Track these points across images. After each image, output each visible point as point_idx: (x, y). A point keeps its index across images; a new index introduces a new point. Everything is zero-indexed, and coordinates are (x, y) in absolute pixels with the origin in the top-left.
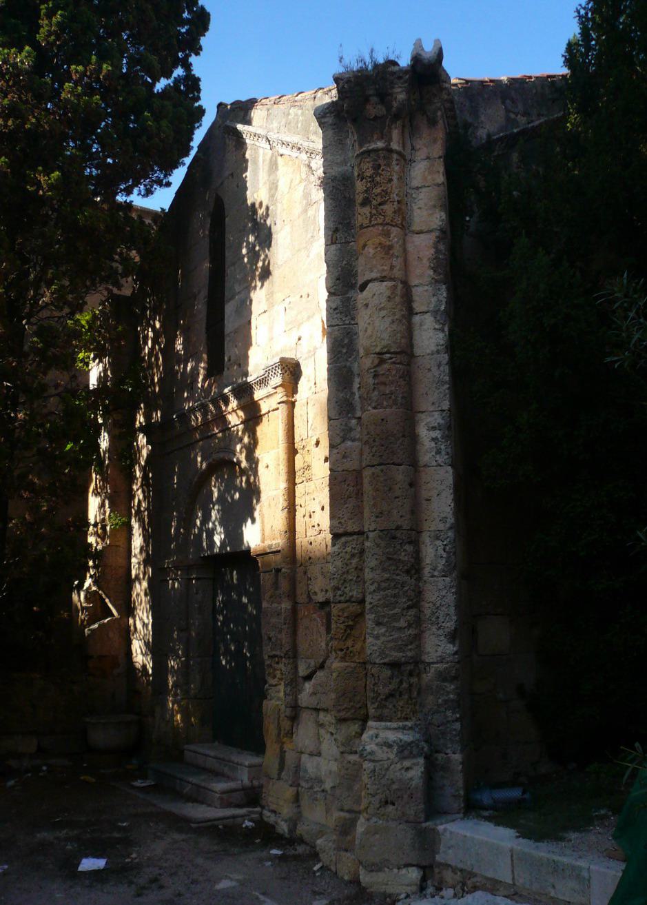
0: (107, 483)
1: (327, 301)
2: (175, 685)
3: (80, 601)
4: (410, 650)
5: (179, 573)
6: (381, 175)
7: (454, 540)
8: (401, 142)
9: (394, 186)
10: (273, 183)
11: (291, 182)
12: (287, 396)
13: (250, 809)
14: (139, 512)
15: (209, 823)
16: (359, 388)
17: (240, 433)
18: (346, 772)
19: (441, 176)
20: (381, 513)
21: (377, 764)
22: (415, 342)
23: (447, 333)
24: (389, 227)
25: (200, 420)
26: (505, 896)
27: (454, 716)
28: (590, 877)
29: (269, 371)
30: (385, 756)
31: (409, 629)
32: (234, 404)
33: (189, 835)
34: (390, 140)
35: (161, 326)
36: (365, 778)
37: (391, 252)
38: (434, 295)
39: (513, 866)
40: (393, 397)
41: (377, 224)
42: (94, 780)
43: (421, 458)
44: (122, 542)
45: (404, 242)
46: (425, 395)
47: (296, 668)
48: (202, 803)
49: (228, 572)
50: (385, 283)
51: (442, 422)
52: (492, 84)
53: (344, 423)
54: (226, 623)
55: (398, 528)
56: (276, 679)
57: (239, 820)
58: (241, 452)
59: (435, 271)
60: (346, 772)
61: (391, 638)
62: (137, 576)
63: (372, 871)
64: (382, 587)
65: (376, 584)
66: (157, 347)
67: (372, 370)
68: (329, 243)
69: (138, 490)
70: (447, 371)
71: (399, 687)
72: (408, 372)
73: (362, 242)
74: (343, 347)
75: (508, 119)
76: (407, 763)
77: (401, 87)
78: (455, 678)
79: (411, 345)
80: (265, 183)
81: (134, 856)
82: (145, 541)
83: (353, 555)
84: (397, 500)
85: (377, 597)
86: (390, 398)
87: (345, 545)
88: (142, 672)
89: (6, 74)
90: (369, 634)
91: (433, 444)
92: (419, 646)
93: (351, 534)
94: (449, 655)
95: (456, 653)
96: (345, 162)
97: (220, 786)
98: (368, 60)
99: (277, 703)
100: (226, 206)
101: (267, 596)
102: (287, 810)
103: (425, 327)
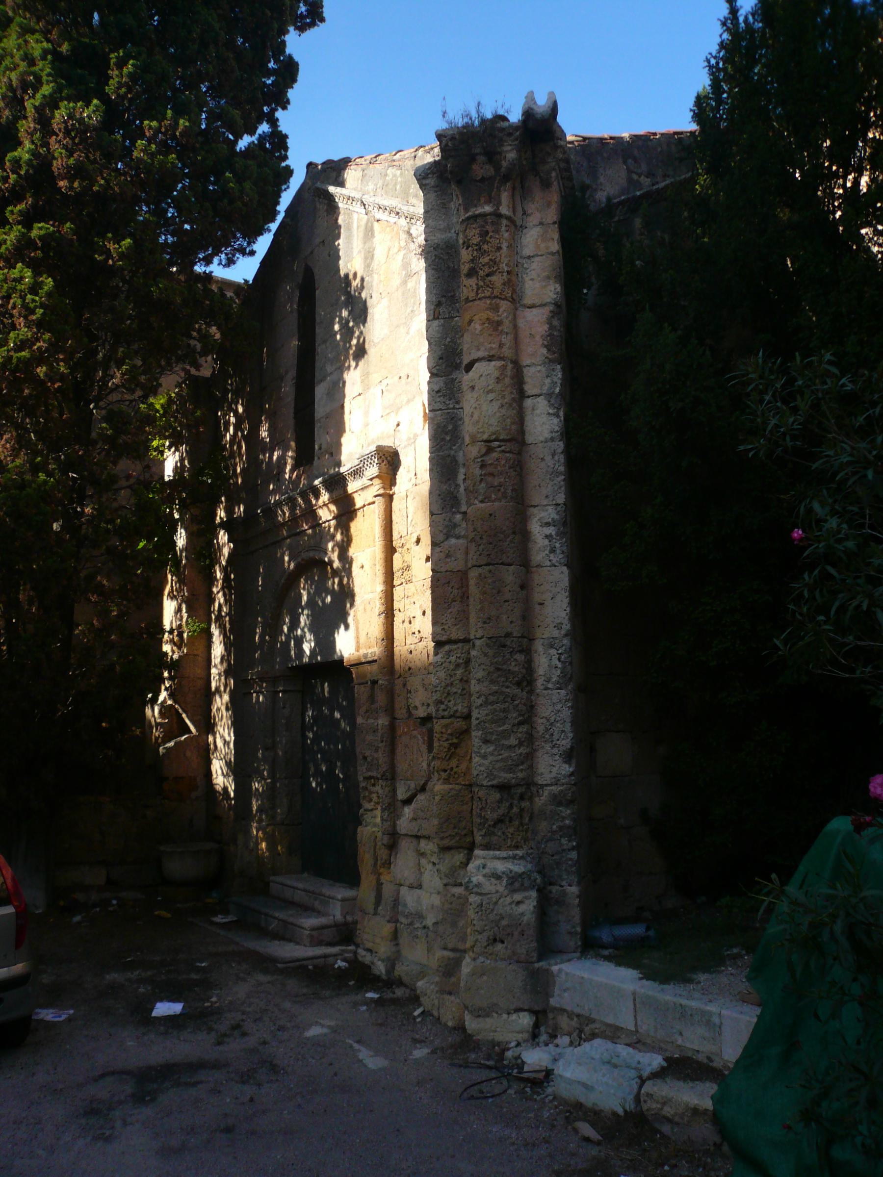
0: (185, 584)
1: (429, 383)
2: (260, 810)
3: (153, 715)
4: (522, 770)
6: (488, 242)
7: (570, 649)
8: (511, 206)
9: (503, 255)
10: (369, 252)
11: (389, 250)
12: (384, 488)
13: (344, 948)
14: (219, 618)
16: (465, 479)
17: (332, 530)
20: (489, 619)
21: (485, 898)
23: (562, 418)
24: (498, 301)
25: (287, 515)
28: (721, 1023)
29: (364, 460)
30: (493, 889)
32: (325, 497)
34: (499, 204)
35: (244, 411)
36: (471, 913)
37: (500, 328)
38: (547, 376)
41: (485, 297)
42: (169, 916)
43: (533, 558)
44: (200, 649)
45: (515, 317)
46: (538, 487)
47: (394, 791)
48: (290, 940)
49: (319, 685)
50: (493, 363)
51: (556, 517)
52: (612, 141)
53: (447, 519)
55: (508, 635)
56: (372, 803)
57: (331, 960)
59: (549, 350)
61: (500, 757)
62: (217, 689)
63: (479, 1016)
64: (490, 701)
65: (483, 698)
66: (240, 434)
67: (479, 460)
68: (431, 318)
69: (218, 592)
70: (562, 460)
71: (509, 812)
73: (467, 318)
74: (447, 434)
75: (630, 180)
76: (518, 897)
78: (570, 803)
79: (522, 432)
80: (360, 252)
81: (214, 999)
82: (226, 649)
83: (458, 666)
84: (507, 603)
85: (484, 712)
86: (499, 490)
88: (223, 795)
90: (475, 752)
91: (546, 542)
92: (531, 767)
93: (456, 642)
94: (564, 776)
95: (572, 774)
96: (448, 228)
97: (310, 922)
99: (374, 829)
102: (384, 949)
103: (538, 412)
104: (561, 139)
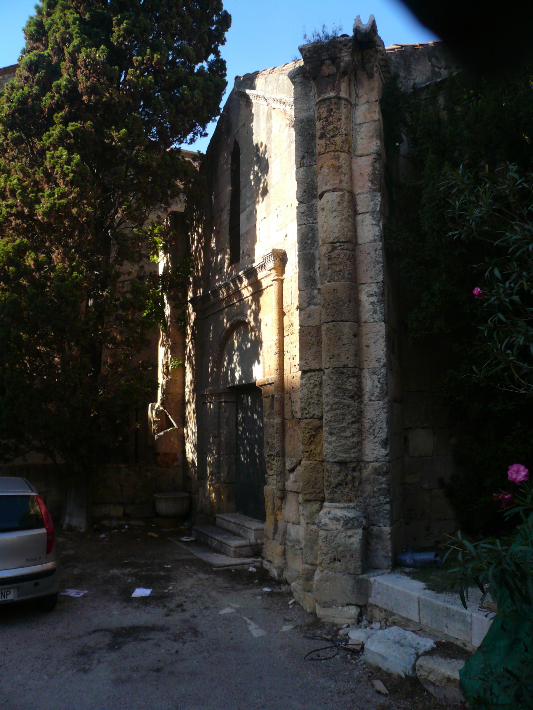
0: (170, 338)
1: (297, 207)
2: (211, 474)
3: (152, 416)
4: (354, 452)
5: (214, 398)
6: (333, 116)
7: (386, 375)
8: (348, 91)
10: (269, 129)
11: (281, 126)
12: (278, 276)
13: (254, 559)
14: (189, 357)
15: (225, 568)
16: (319, 268)
17: (250, 302)
18: (309, 537)
19: (377, 114)
20: (333, 356)
21: (329, 532)
22: (358, 234)
25: (225, 294)
26: (413, 631)
27: (385, 500)
28: (472, 622)
29: (265, 258)
30: (334, 527)
31: (352, 438)
32: (245, 282)
33: (211, 576)
34: (339, 90)
35: (202, 232)
36: (320, 542)
37: (340, 171)
38: (372, 200)
39: (419, 610)
40: (342, 274)
41: (330, 151)
42: (157, 536)
43: (362, 317)
44: (179, 377)
45: (351, 163)
46: (365, 272)
47: (284, 464)
48: (223, 553)
49: (245, 398)
50: (336, 193)
51: (377, 290)
52: (421, 47)
53: (309, 293)
54: (244, 431)
55: (345, 366)
56: (273, 471)
57: (246, 567)
58: (250, 315)
59: (372, 183)
60: (309, 537)
61: (340, 444)
62: (189, 400)
63: (324, 607)
64: (334, 408)
65: (329, 406)
66: (200, 246)
67: (327, 255)
68: (299, 166)
69: (189, 342)
70: (381, 254)
71: (345, 479)
72: (353, 255)
73: (319, 165)
74: (308, 239)
75: (434, 72)
76: (350, 533)
77: (346, 52)
78: (386, 473)
79: (355, 236)
81: (170, 588)
82: (193, 377)
83: (315, 386)
85: (330, 415)
86: (340, 274)
87: (310, 378)
88: (192, 464)
89: (89, 65)
90: (325, 441)
91: (371, 306)
92: (360, 450)
93: (314, 371)
95: (387, 455)
96: (309, 109)
97: (235, 543)
98: (321, 34)
99: (273, 487)
100: (240, 147)
101: (266, 414)
102: (278, 561)
103: (366, 223)
104: (380, 46)
